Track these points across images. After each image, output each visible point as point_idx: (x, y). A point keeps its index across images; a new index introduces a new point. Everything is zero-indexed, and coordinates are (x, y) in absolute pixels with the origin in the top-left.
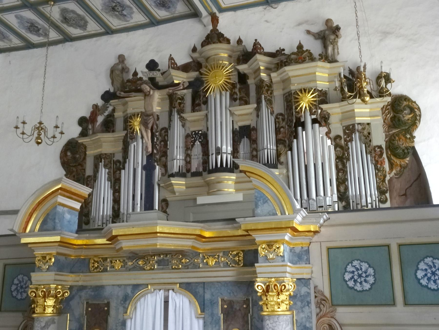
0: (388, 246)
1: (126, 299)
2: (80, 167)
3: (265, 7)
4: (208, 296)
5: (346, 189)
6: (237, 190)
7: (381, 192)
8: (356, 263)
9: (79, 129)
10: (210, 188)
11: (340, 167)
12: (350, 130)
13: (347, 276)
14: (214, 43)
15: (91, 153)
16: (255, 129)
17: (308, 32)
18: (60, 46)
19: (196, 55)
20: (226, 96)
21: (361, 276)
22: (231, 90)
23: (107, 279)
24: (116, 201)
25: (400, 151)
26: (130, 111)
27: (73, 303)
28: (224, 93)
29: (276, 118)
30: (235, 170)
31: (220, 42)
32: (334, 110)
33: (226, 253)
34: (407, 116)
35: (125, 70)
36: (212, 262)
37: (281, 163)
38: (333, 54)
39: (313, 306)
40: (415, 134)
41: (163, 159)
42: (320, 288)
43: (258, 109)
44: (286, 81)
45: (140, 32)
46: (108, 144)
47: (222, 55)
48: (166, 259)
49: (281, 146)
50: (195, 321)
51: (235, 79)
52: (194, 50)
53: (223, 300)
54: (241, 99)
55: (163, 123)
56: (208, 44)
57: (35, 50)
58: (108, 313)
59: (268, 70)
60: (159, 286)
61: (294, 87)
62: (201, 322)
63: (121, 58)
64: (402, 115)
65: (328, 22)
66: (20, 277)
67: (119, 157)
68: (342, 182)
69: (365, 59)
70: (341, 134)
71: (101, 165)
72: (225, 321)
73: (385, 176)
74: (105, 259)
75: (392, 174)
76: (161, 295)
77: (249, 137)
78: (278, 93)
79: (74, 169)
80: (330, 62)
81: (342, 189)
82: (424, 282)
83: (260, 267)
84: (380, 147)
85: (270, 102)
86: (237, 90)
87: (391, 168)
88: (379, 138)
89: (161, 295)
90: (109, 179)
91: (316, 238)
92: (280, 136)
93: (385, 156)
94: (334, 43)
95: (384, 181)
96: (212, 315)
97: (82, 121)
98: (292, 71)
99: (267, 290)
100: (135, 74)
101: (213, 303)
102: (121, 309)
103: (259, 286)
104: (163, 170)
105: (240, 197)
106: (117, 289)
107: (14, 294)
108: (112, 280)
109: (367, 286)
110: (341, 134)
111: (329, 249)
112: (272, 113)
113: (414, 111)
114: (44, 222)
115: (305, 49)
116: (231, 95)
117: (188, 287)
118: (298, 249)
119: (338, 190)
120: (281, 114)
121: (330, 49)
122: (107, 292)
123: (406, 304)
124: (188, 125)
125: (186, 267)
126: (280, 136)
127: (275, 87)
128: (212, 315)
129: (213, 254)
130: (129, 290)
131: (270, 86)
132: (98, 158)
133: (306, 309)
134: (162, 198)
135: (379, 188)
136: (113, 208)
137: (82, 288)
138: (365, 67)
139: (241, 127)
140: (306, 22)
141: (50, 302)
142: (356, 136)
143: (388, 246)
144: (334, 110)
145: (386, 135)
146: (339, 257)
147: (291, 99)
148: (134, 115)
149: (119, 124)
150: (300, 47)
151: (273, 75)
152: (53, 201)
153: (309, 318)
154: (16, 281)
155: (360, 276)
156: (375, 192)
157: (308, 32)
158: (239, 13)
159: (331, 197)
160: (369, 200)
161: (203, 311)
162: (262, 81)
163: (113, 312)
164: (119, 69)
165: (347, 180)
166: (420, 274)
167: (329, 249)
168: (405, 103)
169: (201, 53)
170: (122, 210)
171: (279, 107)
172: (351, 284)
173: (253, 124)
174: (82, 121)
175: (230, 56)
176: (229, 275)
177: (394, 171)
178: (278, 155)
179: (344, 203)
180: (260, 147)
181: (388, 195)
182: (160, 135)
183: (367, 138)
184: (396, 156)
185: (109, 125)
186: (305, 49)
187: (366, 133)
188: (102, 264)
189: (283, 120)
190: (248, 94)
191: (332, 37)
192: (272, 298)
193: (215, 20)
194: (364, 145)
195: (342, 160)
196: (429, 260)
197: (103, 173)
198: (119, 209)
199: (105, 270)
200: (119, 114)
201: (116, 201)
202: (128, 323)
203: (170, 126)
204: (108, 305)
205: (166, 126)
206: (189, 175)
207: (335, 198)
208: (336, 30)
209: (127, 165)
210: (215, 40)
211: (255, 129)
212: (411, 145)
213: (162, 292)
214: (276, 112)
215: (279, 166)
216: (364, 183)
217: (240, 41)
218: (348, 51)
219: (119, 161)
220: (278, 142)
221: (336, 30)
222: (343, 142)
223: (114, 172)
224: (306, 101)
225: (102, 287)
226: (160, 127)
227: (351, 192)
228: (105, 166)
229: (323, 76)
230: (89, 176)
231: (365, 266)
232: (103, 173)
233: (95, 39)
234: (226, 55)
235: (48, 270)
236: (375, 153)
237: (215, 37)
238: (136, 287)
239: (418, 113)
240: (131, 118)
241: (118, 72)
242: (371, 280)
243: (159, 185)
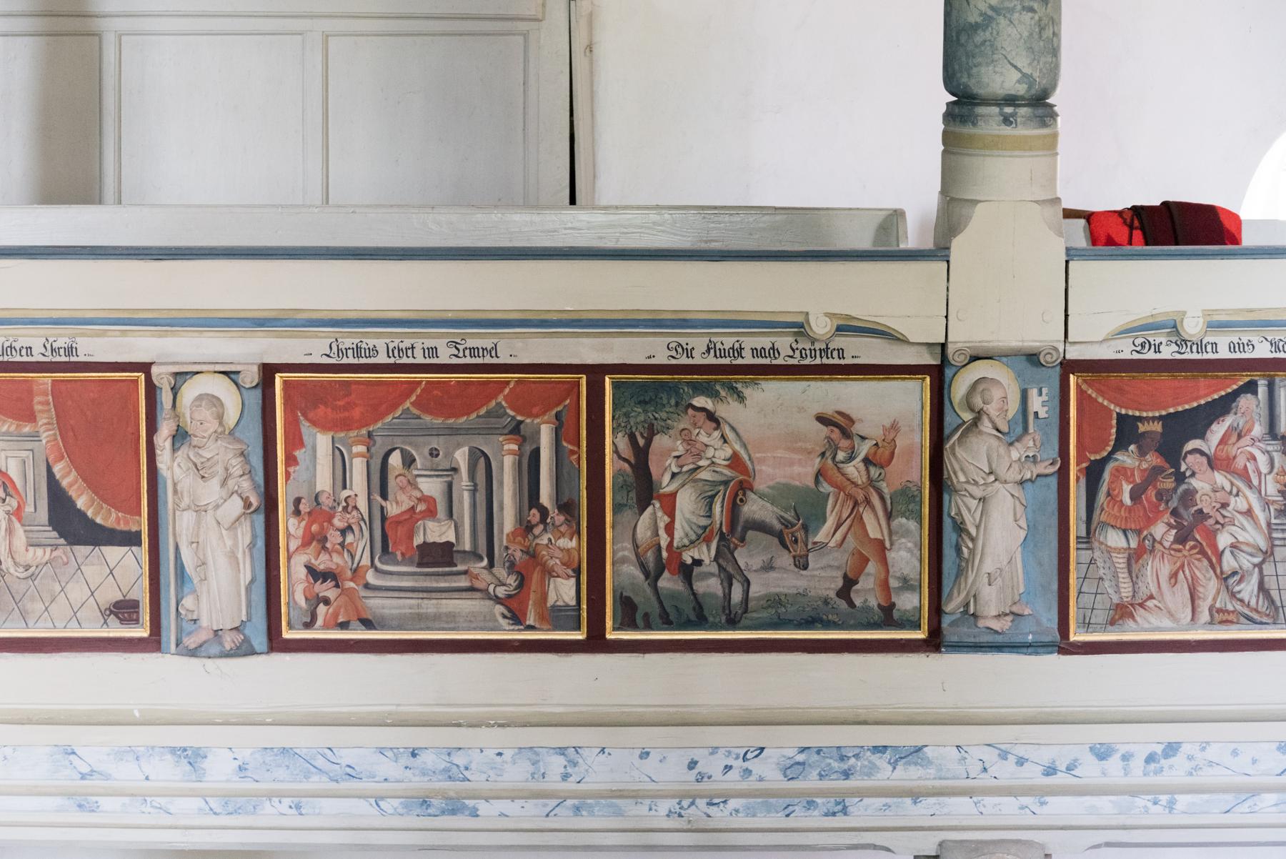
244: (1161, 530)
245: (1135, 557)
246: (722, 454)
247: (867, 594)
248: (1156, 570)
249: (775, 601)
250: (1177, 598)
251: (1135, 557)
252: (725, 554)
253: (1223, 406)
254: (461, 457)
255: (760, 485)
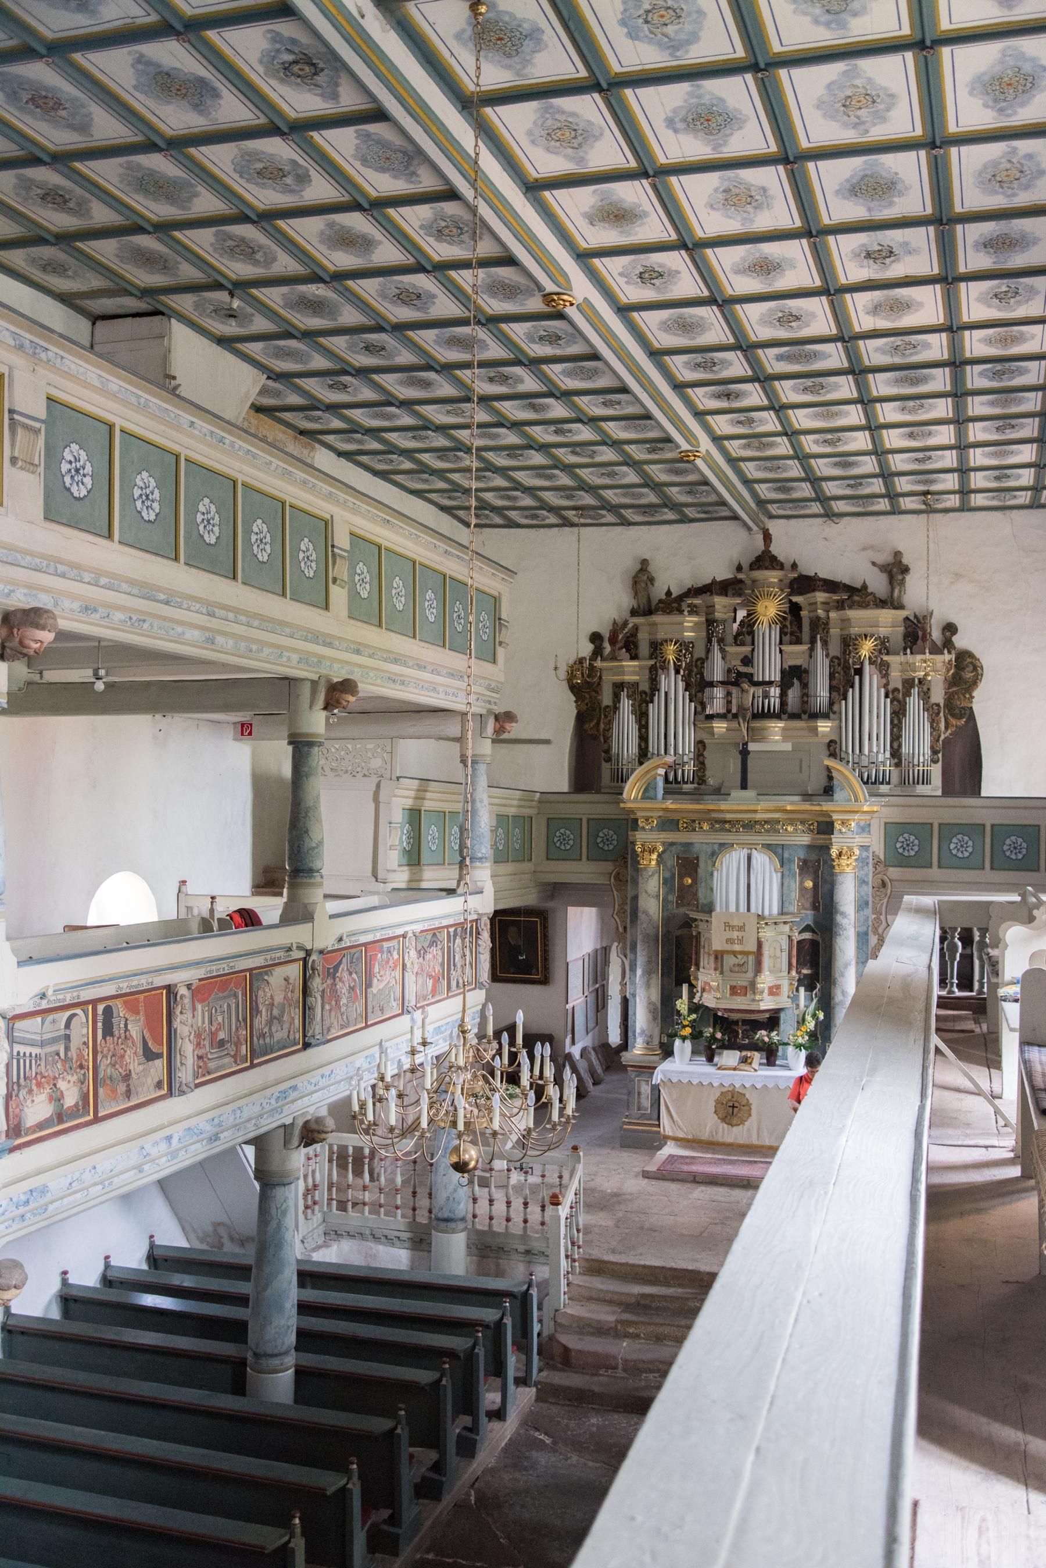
0: (932, 824)
1: (714, 855)
2: (593, 694)
3: (825, 519)
4: (786, 855)
5: (900, 746)
6: (785, 738)
7: (934, 752)
8: (906, 835)
9: (590, 647)
10: (755, 735)
11: (896, 722)
12: (908, 684)
13: (898, 845)
14: (767, 568)
15: (609, 679)
16: (806, 671)
17: (874, 564)
18: (556, 529)
19: (740, 576)
20: (776, 630)
21: (908, 845)
22: (781, 623)
23: (694, 838)
24: (643, 738)
25: (957, 711)
26: (661, 636)
27: (665, 856)
28: (773, 626)
29: (831, 661)
30: (783, 716)
31: (774, 568)
32: (895, 660)
33: (803, 822)
34: (968, 675)
35: (652, 580)
36: (790, 829)
37: (834, 713)
38: (900, 597)
39: (871, 866)
40: (974, 694)
41: (700, 695)
42: (877, 853)
43: (812, 649)
44: (845, 622)
45: (666, 527)
46: (631, 670)
47: (772, 580)
48: (749, 826)
49: (834, 694)
50: (774, 874)
51: (786, 607)
52: (739, 568)
53: (799, 859)
54: (792, 634)
55: (699, 652)
56: (758, 568)
57: (519, 530)
58: (697, 864)
59: (827, 606)
60: (743, 845)
61: (854, 631)
62: (779, 874)
63: (644, 563)
64: (965, 672)
65: (897, 554)
66: (605, 831)
67: (645, 687)
68: (896, 738)
69: (933, 605)
70: (900, 688)
71: (624, 695)
72: (800, 874)
73: (939, 736)
74: (694, 821)
75: (947, 734)
76: (745, 851)
77: (800, 679)
78: (835, 631)
79: (587, 696)
80: (895, 608)
81: (895, 745)
82: (954, 852)
83: (835, 838)
84: (938, 705)
85: (825, 643)
86: (788, 623)
87: (946, 728)
88: (938, 696)
89: (745, 851)
90: (634, 712)
91: (876, 815)
92: (834, 683)
93: (942, 714)
94: (902, 582)
95: (938, 740)
96: (790, 870)
97: (596, 638)
98: (854, 614)
99: (840, 854)
100: (669, 593)
101: (790, 861)
102: (710, 863)
103: (834, 852)
104: (699, 709)
105: (788, 747)
106: (705, 847)
107: (601, 845)
108: (701, 839)
109: (912, 853)
110: (900, 688)
111: (886, 823)
112: (827, 656)
113: (977, 668)
114: (646, 790)
115: (870, 590)
116: (781, 629)
117: (768, 847)
118: (862, 823)
119: (891, 747)
120: (837, 658)
121: (896, 592)
122: (696, 848)
123: (939, 867)
124: (728, 658)
125: (768, 831)
126: (834, 683)
127: (831, 625)
128: (790, 870)
129: (791, 822)
130: (716, 847)
131: (827, 624)
132: (619, 687)
133: (866, 868)
134: (698, 739)
135: (932, 748)
136: (640, 745)
137: (672, 844)
138: (932, 613)
139: (790, 667)
140: (872, 547)
141: (654, 856)
142: (915, 691)
143: (932, 824)
144: (895, 660)
145: (946, 693)
146: (894, 831)
147: (849, 643)
148: (666, 641)
149: (644, 649)
150: (865, 587)
151: (833, 615)
152: (653, 773)
153: (867, 875)
154: (601, 834)
155: (908, 845)
156: (928, 751)
157: (874, 564)
158: (793, 522)
159: (884, 756)
160: (921, 760)
161: (782, 866)
162: (818, 618)
163: (702, 864)
164: (642, 576)
165: (901, 736)
166: (952, 846)
167: (886, 823)
168: (969, 660)
169: (748, 576)
170: (651, 749)
171: (835, 649)
172: (901, 850)
173: (805, 666)
174: (596, 638)
175: (781, 580)
176: (805, 839)
177: (949, 731)
178: (831, 703)
179: (896, 760)
180: (811, 692)
181: (940, 755)
182: (696, 666)
183: (925, 695)
184: (953, 716)
185: (631, 646)
186: (870, 590)
187: (925, 688)
188: (692, 825)
189: (839, 664)
190: (800, 628)
191: (900, 577)
192: (844, 861)
193: (767, 537)
194: (921, 702)
195: (898, 714)
196: (960, 836)
197: (626, 705)
198: (647, 747)
199: (695, 830)
200: (643, 637)
201: (643, 738)
202: (715, 873)
203: (707, 658)
204: (697, 858)
205: (703, 656)
206: (730, 716)
207: (888, 754)
208: (905, 570)
209: (656, 698)
210: (767, 563)
211: (806, 671)
212: (969, 705)
213: (745, 850)
214: (832, 653)
215: (831, 715)
216: (919, 740)
217: (794, 566)
218: (916, 593)
219: (644, 692)
220: (832, 688)
221: (905, 570)
222: (901, 695)
223: (640, 706)
224: (866, 648)
225: (692, 844)
226: (696, 656)
227: (904, 750)
228: (629, 697)
229: (887, 622)
230: (607, 707)
231: (912, 838)
232: (626, 705)
233: (604, 528)
234: (776, 580)
235: (651, 830)
236: (932, 711)
237: (766, 560)
238: (722, 845)
239: (980, 671)
240: (662, 644)
241: (643, 585)
242: (916, 848)
243: (695, 724)
244: (333, 1003)
245: (330, 1010)
246: (269, 995)
247: (292, 1037)
248: (333, 1013)
249: (278, 1042)
250: (335, 1023)
251: (330, 1010)
252: (270, 1029)
253: (340, 962)
254: (225, 1006)
255: (276, 1004)
